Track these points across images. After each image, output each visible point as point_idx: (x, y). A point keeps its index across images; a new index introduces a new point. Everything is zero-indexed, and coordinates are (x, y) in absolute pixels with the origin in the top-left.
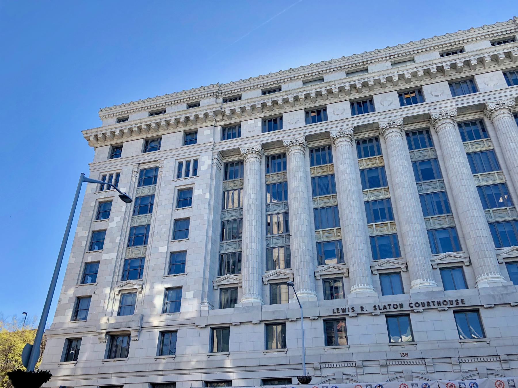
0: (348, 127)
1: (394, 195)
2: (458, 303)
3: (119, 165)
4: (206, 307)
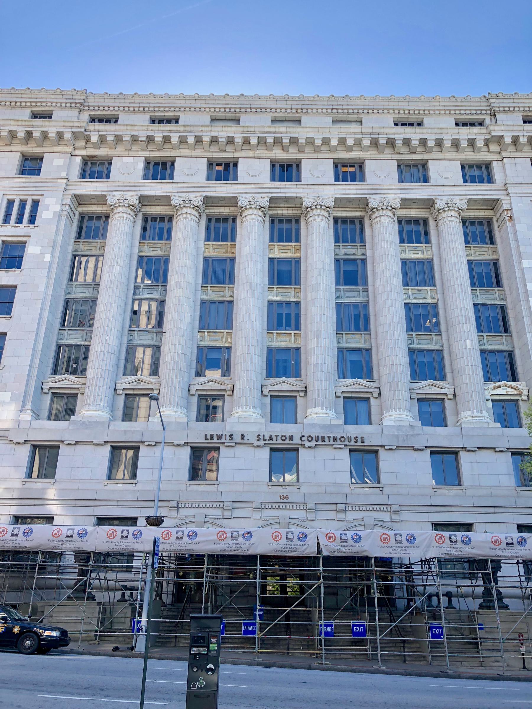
0: (263, 195)
1: (306, 299)
2: (356, 441)
4: (27, 416)
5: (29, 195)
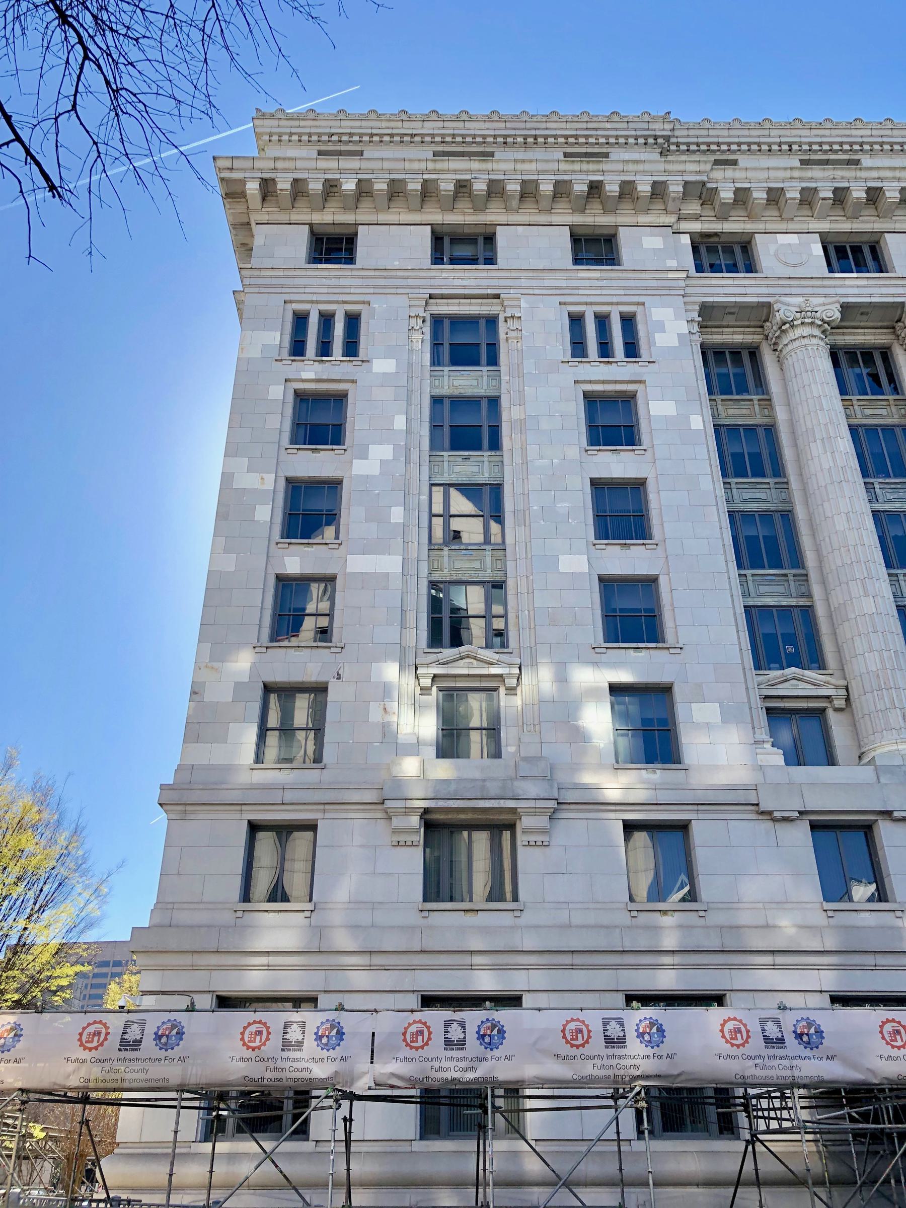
3: (361, 287)
4: (777, 758)
5: (611, 304)
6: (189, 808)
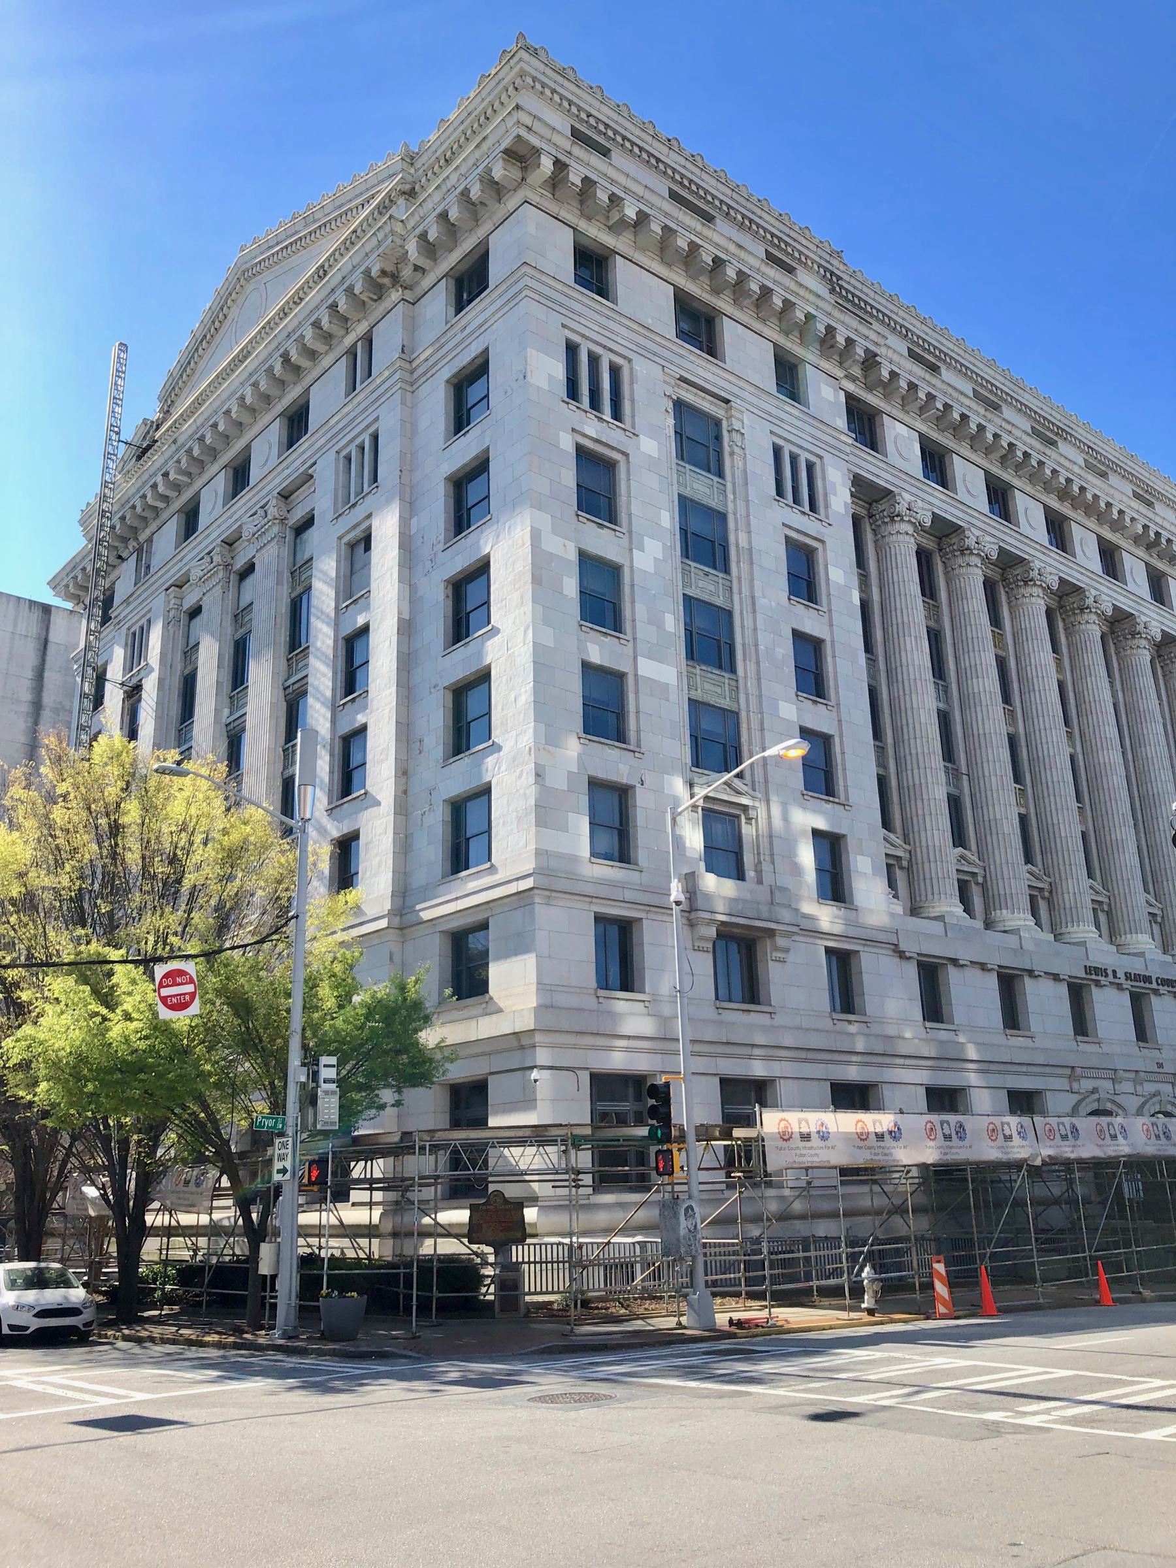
6: (554, 894)
